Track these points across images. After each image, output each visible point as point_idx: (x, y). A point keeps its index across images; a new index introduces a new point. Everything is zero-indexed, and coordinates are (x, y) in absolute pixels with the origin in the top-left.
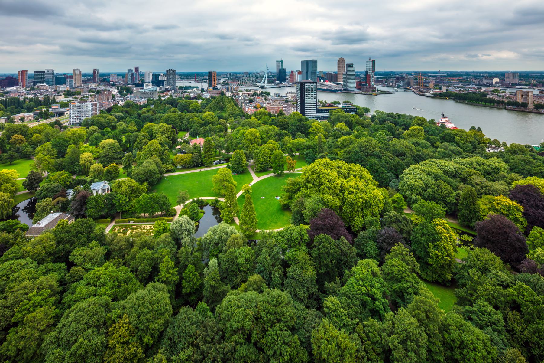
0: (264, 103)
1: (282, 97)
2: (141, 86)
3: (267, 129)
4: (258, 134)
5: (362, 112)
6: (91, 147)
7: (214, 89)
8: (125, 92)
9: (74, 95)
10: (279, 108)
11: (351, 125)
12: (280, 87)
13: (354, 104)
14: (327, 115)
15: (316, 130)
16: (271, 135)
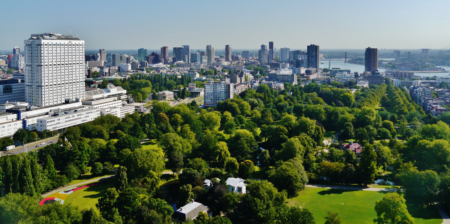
2: (276, 66)
7: (373, 73)
8: (258, 74)
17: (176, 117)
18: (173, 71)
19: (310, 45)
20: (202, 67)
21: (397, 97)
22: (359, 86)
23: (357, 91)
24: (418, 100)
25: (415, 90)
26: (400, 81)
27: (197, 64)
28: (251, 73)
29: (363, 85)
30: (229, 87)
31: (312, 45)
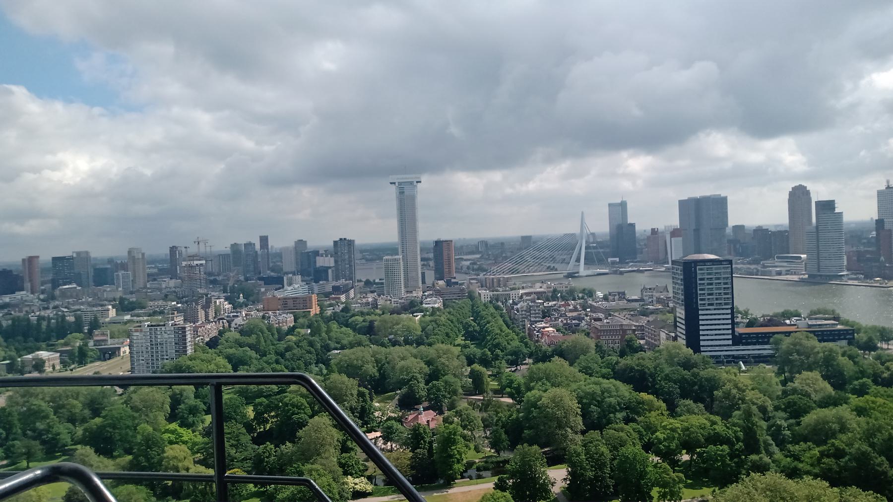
0: (580, 319)
1: (629, 301)
2: (277, 282)
3: (598, 390)
4: (575, 405)
5: (870, 339)
6: (181, 430)
7: (449, 283)
9: (133, 309)
10: (624, 331)
11: (837, 379)
12: (622, 273)
13: (844, 316)
14: (766, 350)
15: (734, 391)
16: (610, 405)
17: (68, 407)
18: (55, 307)
19: (338, 239)
20: (118, 295)
21: (488, 322)
22: (427, 308)
23: (423, 316)
24: (521, 323)
25: (515, 307)
26: (491, 293)
27: (109, 289)
28: (226, 299)
29: (433, 305)
30: (185, 332)
31: (341, 239)
